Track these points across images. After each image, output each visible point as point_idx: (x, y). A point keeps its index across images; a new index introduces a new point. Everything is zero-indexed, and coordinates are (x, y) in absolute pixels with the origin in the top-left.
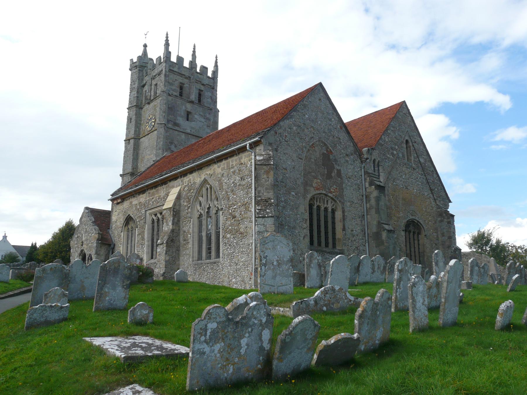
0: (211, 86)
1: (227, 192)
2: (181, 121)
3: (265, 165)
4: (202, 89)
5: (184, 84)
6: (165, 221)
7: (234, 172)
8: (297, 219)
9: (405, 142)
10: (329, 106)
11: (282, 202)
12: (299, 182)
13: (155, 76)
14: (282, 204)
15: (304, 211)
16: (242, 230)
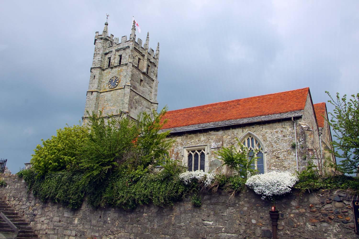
13: (120, 49)
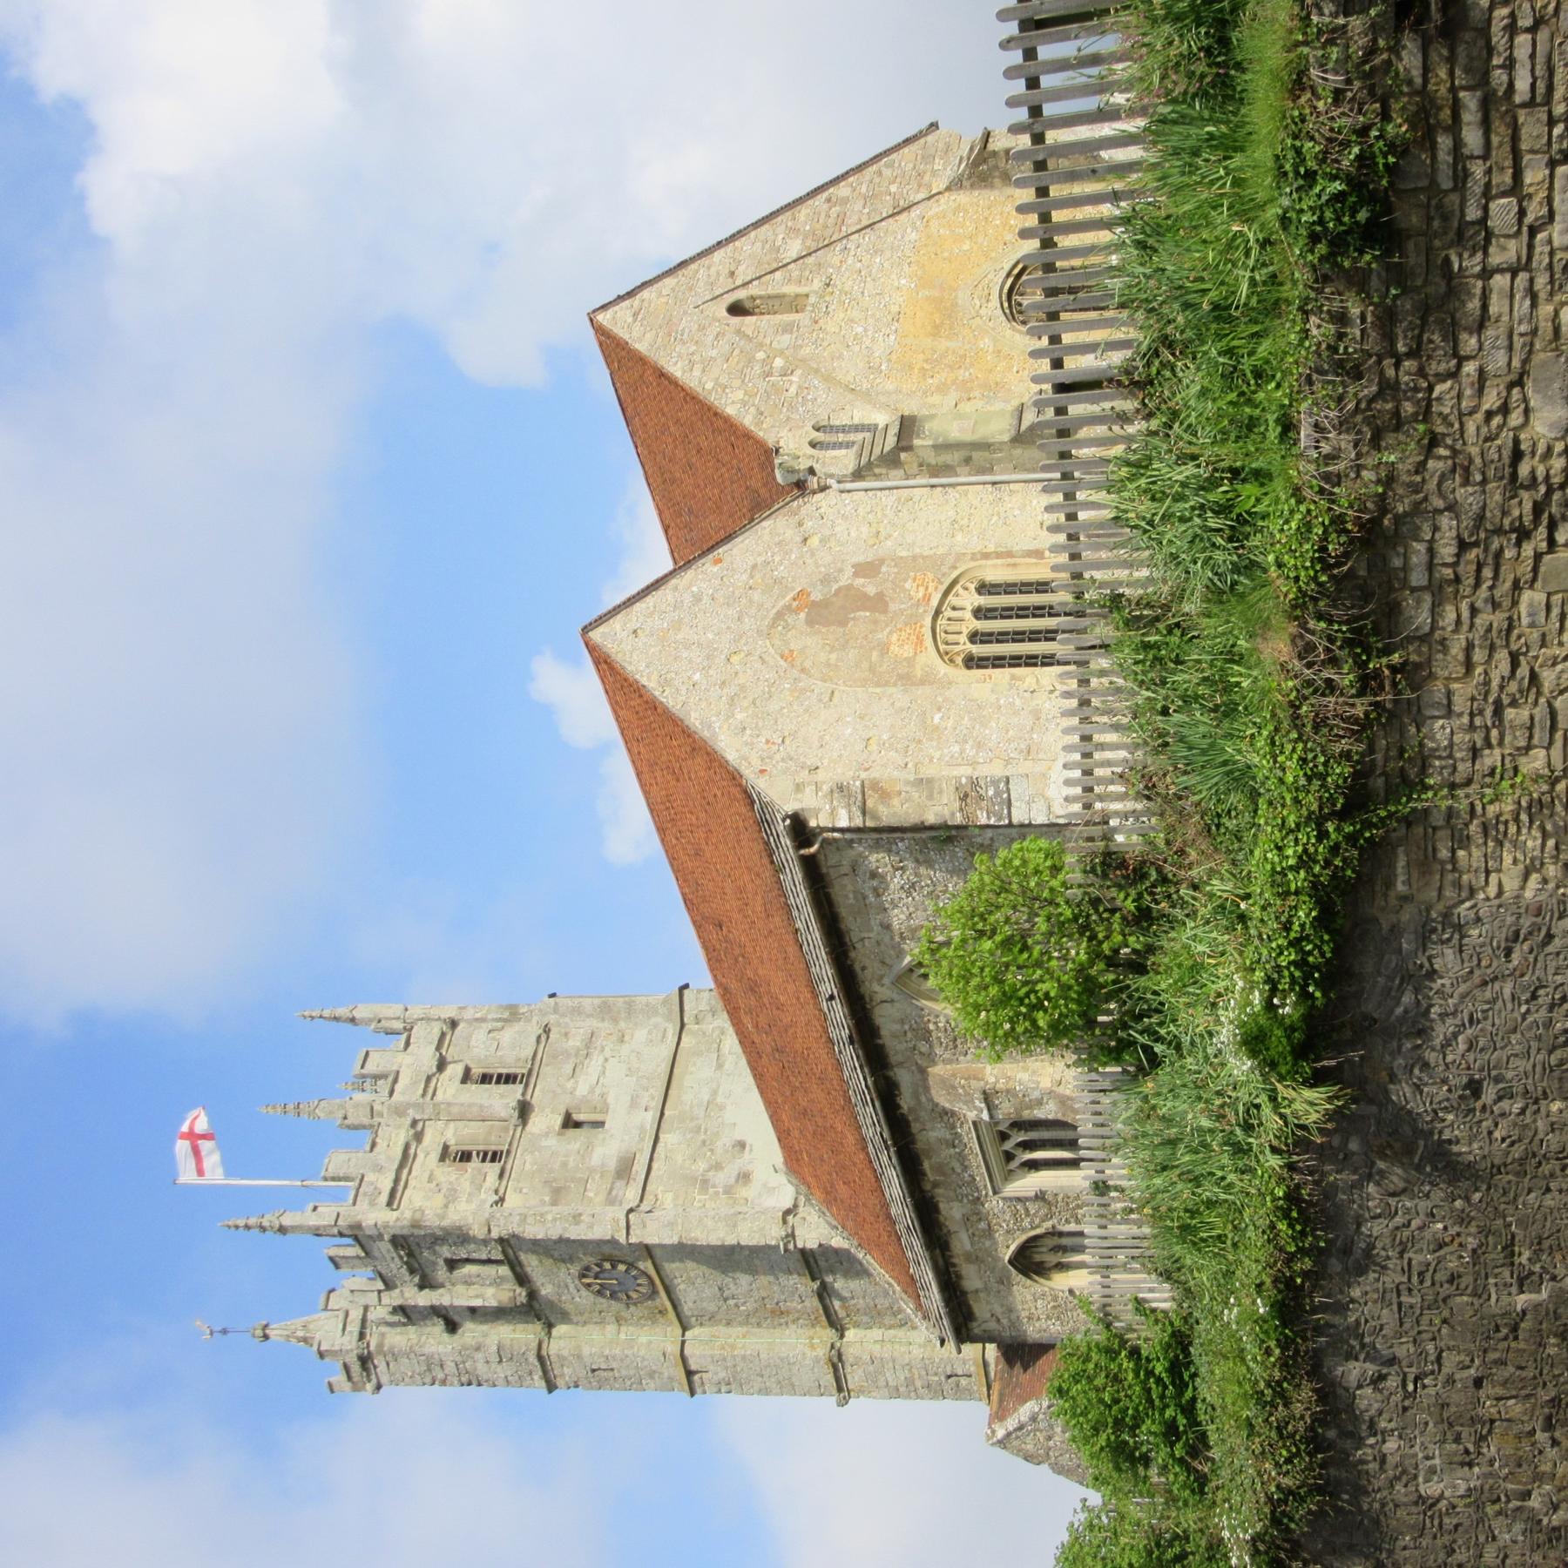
0: (443, 1035)
2: (606, 1149)
5: (446, 1148)
6: (1027, 1115)
9: (736, 320)
10: (650, 600)
13: (412, 1271)
14: (970, 751)
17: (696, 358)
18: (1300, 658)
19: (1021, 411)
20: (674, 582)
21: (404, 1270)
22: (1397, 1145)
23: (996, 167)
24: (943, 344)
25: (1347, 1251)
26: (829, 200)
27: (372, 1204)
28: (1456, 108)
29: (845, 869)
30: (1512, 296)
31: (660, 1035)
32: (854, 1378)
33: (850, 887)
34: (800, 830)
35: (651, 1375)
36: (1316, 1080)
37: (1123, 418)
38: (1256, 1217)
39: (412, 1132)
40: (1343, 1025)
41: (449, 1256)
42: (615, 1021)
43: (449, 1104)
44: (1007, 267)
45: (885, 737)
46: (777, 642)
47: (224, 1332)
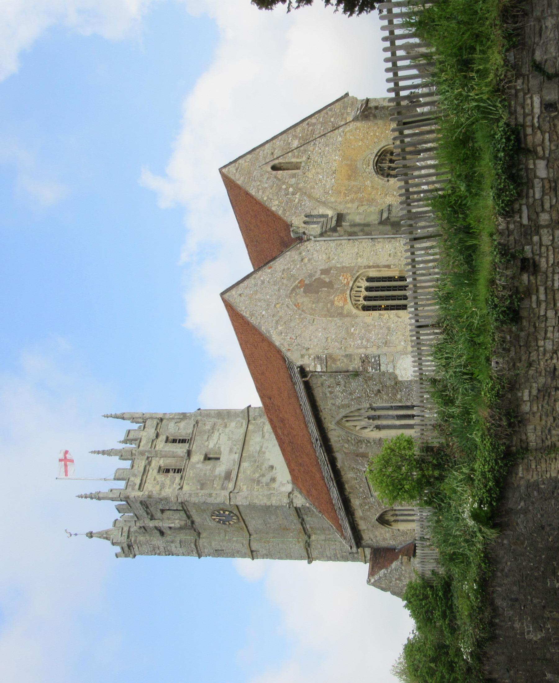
0: (158, 424)
1: (352, 400)
2: (221, 468)
3: (327, 363)
4: (164, 438)
5: (160, 467)
7: (331, 393)
8: (380, 325)
10: (246, 283)
11: (362, 343)
12: (340, 323)
13: (148, 514)
15: (371, 318)
16: (393, 383)
17: (260, 187)
18: (491, 417)
19: (382, 212)
20: (254, 275)
21: (145, 514)
22: (519, 542)
23: (371, 113)
24: (353, 183)
25: (503, 570)
26: (308, 124)
27: (133, 489)
28: (537, 291)
29: (319, 384)
30: (553, 332)
31: (240, 425)
32: (315, 553)
33: (320, 391)
34: (303, 371)
35: (238, 552)
36: (494, 526)
37: (437, 333)
38: (475, 559)
39: (147, 462)
40: (503, 511)
41: (162, 508)
42: (223, 419)
43: (161, 451)
44: (376, 152)
45: (333, 337)
46: (293, 300)
47: (76, 535)
